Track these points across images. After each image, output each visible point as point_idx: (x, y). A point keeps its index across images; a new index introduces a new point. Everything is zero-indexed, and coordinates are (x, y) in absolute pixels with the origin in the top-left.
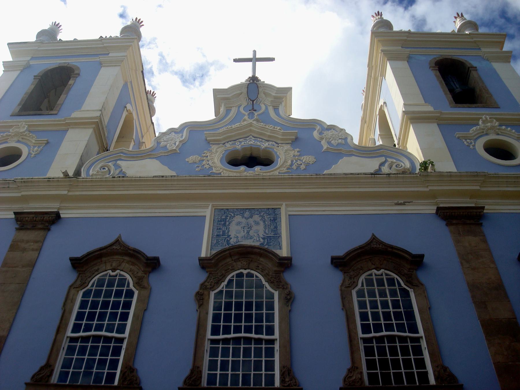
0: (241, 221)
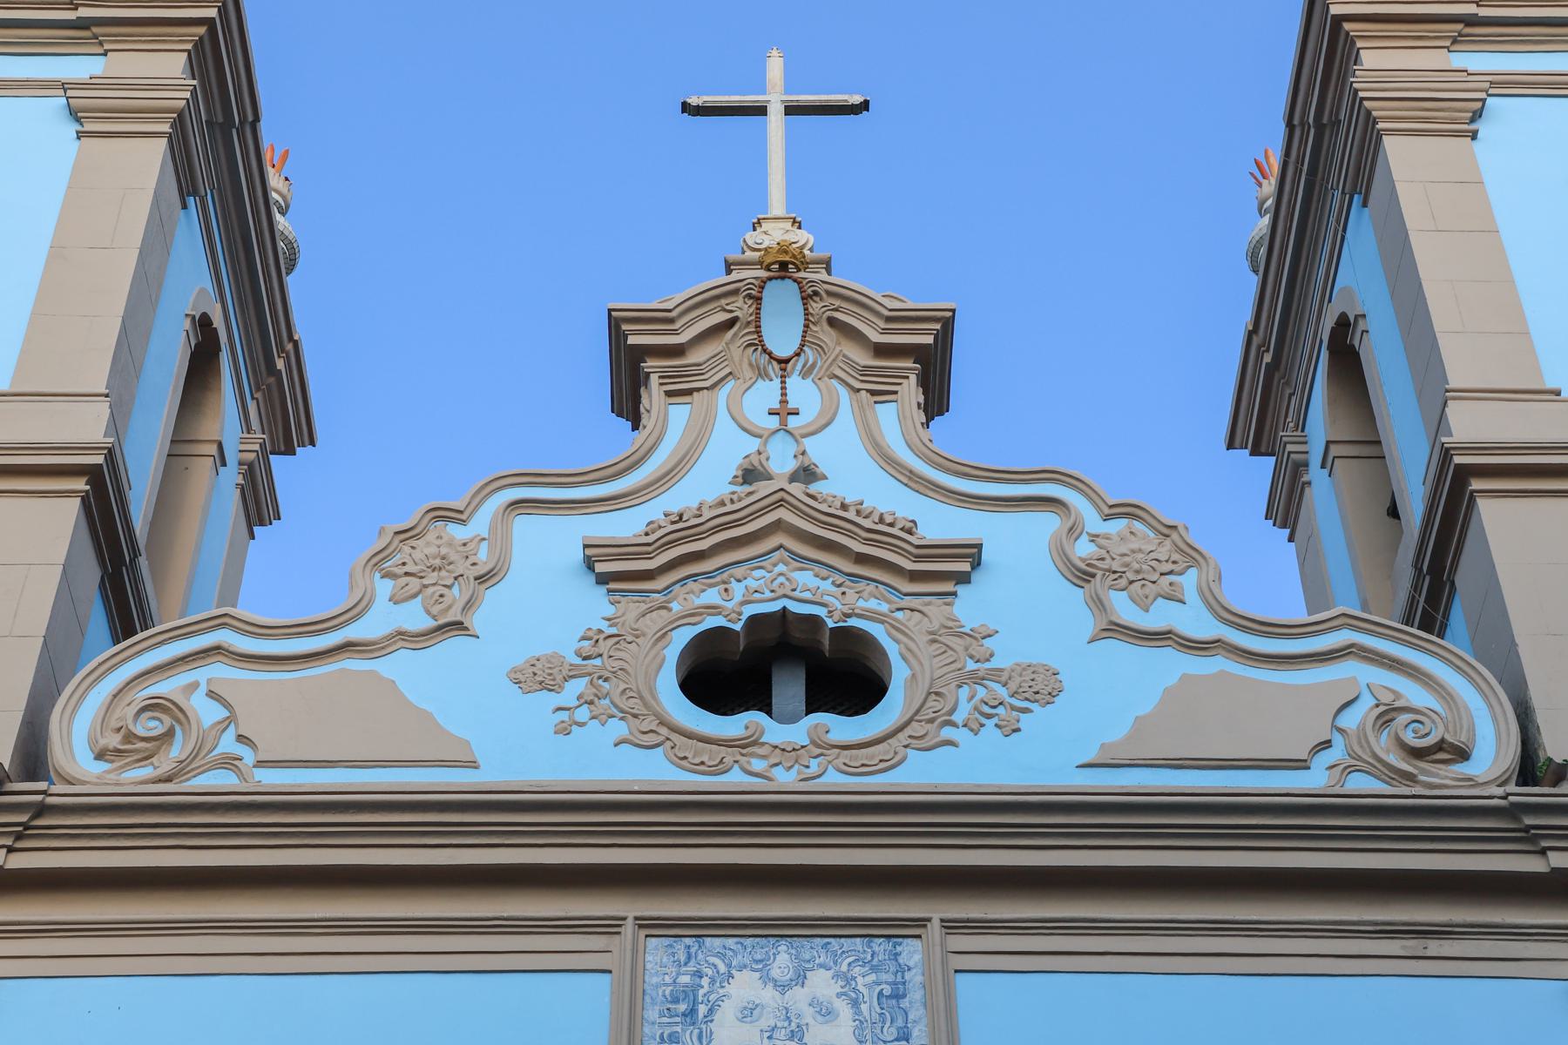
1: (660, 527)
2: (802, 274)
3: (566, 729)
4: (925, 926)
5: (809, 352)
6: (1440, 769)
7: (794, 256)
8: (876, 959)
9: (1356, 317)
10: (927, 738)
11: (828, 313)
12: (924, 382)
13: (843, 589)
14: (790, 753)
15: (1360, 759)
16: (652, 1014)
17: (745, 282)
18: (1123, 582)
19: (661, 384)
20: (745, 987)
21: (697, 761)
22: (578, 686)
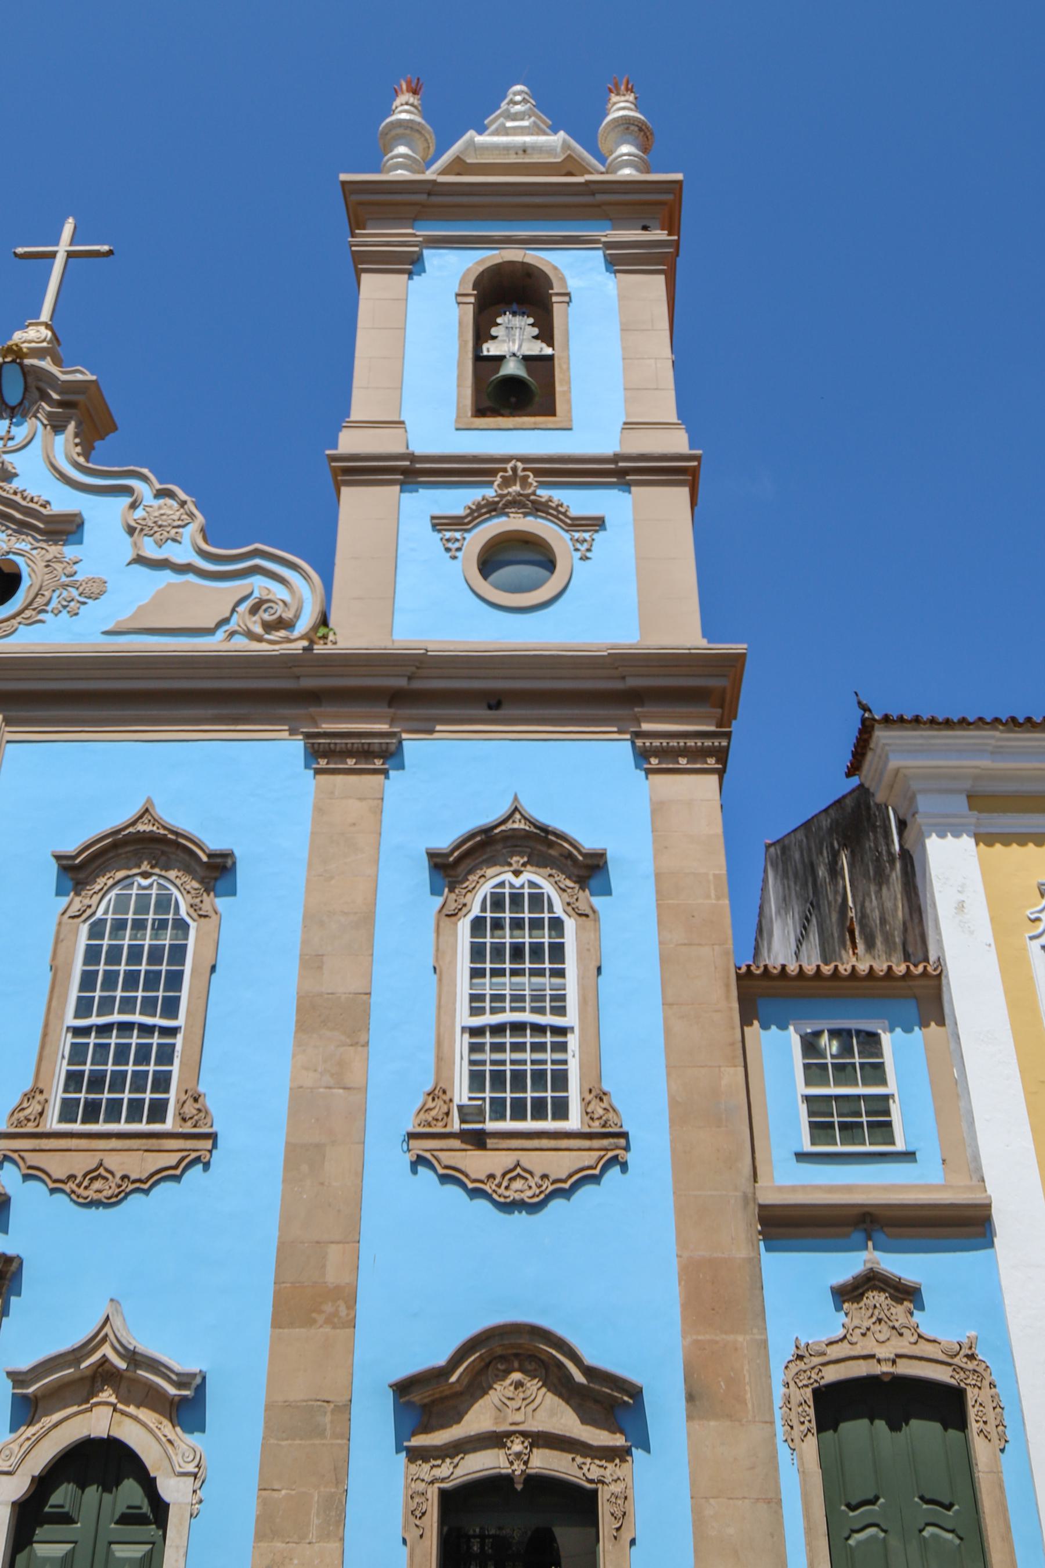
15: (239, 626)
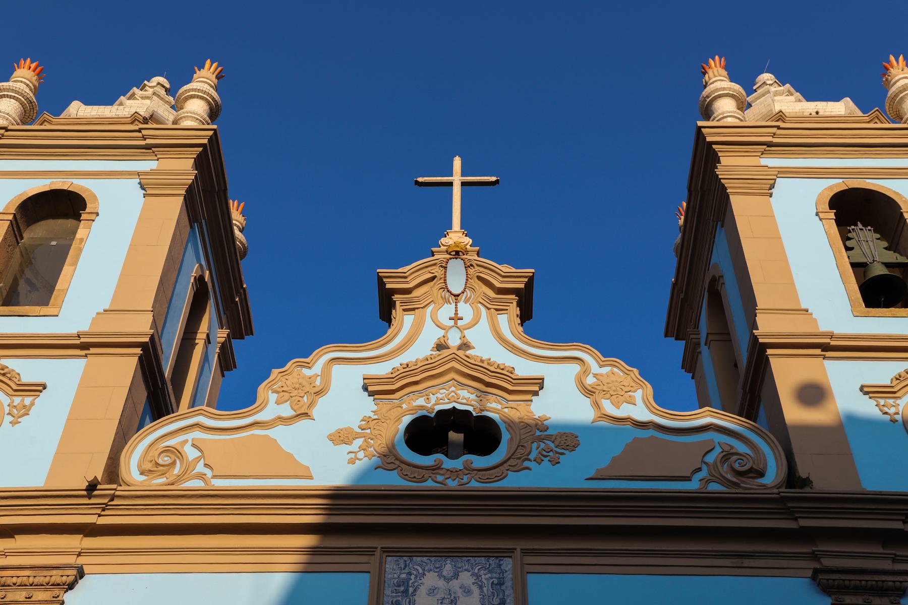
0: (436, 586)
1: (398, 370)
2: (465, 256)
3: (353, 462)
4: (514, 552)
5: (468, 291)
6: (751, 481)
7: (462, 248)
8: (491, 567)
9: (719, 277)
10: (518, 465)
11: (477, 274)
12: (519, 304)
13: (481, 398)
14: (454, 473)
15: (714, 476)
16: (388, 592)
17: (440, 260)
18: (608, 396)
19: (401, 306)
20: (431, 580)
21: (412, 476)
22: (359, 442)
